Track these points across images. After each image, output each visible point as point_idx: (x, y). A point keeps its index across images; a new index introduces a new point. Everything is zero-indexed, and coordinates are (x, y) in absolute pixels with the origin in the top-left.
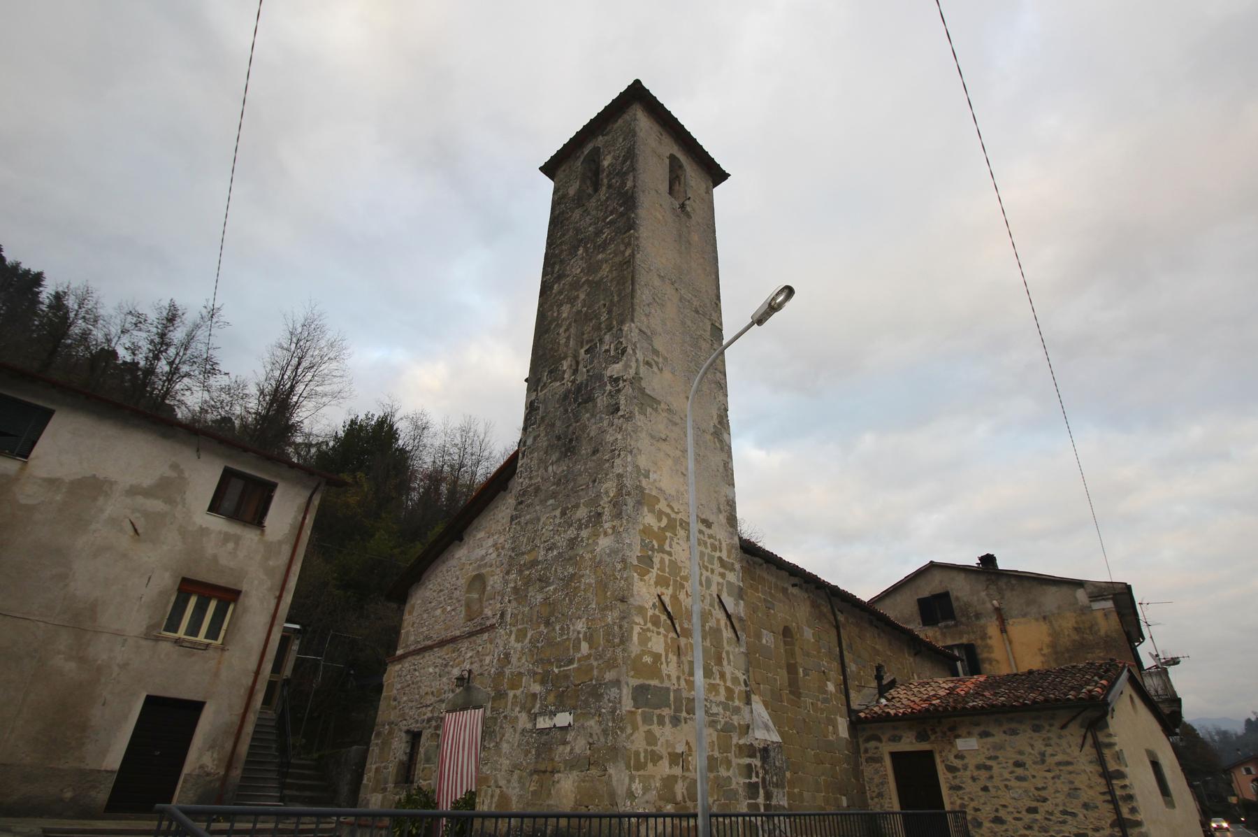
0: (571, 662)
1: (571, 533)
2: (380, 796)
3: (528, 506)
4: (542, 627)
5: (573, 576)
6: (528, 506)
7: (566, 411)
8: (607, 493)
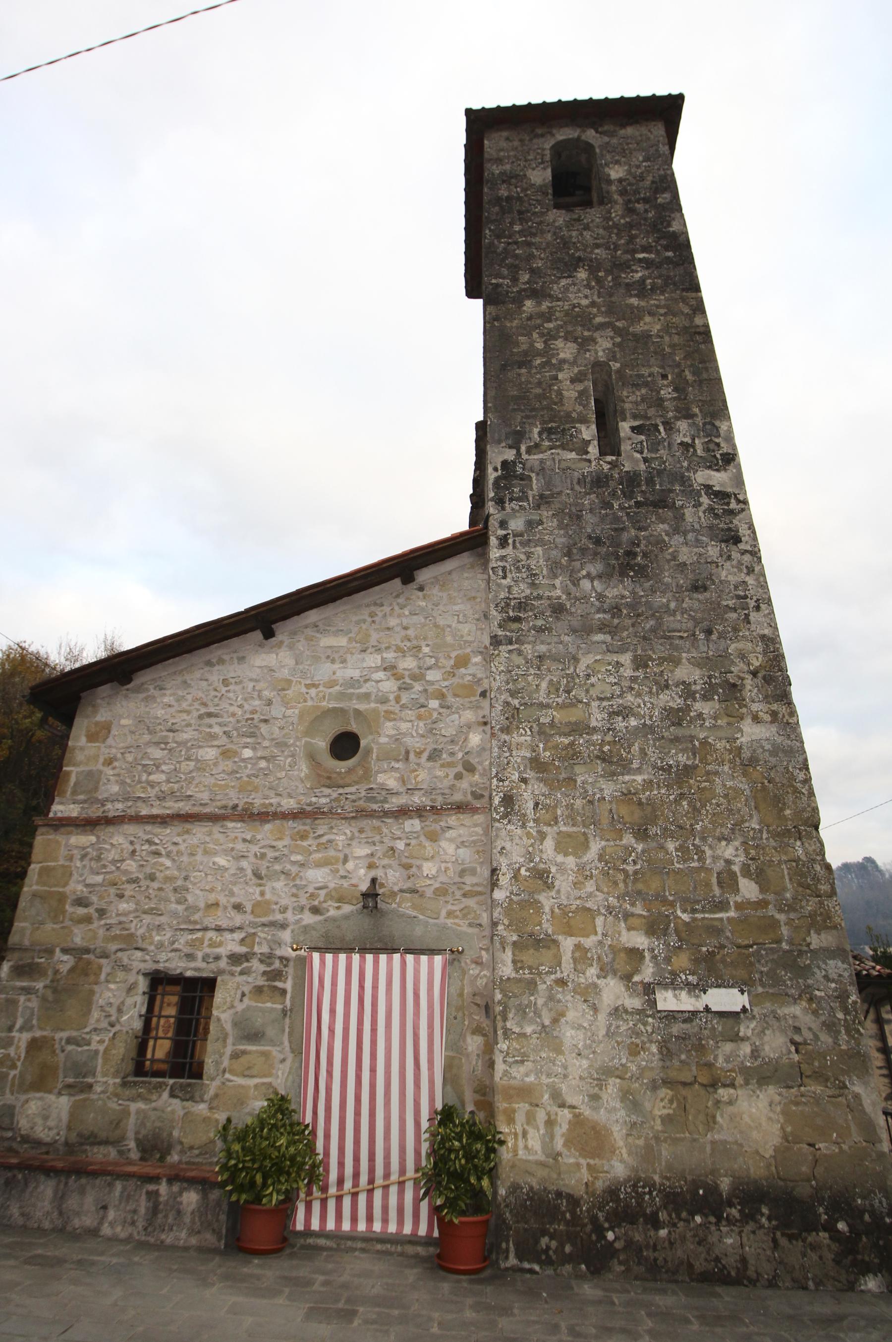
0: (722, 906)
1: (670, 699)
2: (62, 1104)
3: (540, 630)
4: (628, 839)
5: (688, 771)
6: (540, 630)
7: (608, 505)
8: (743, 656)
